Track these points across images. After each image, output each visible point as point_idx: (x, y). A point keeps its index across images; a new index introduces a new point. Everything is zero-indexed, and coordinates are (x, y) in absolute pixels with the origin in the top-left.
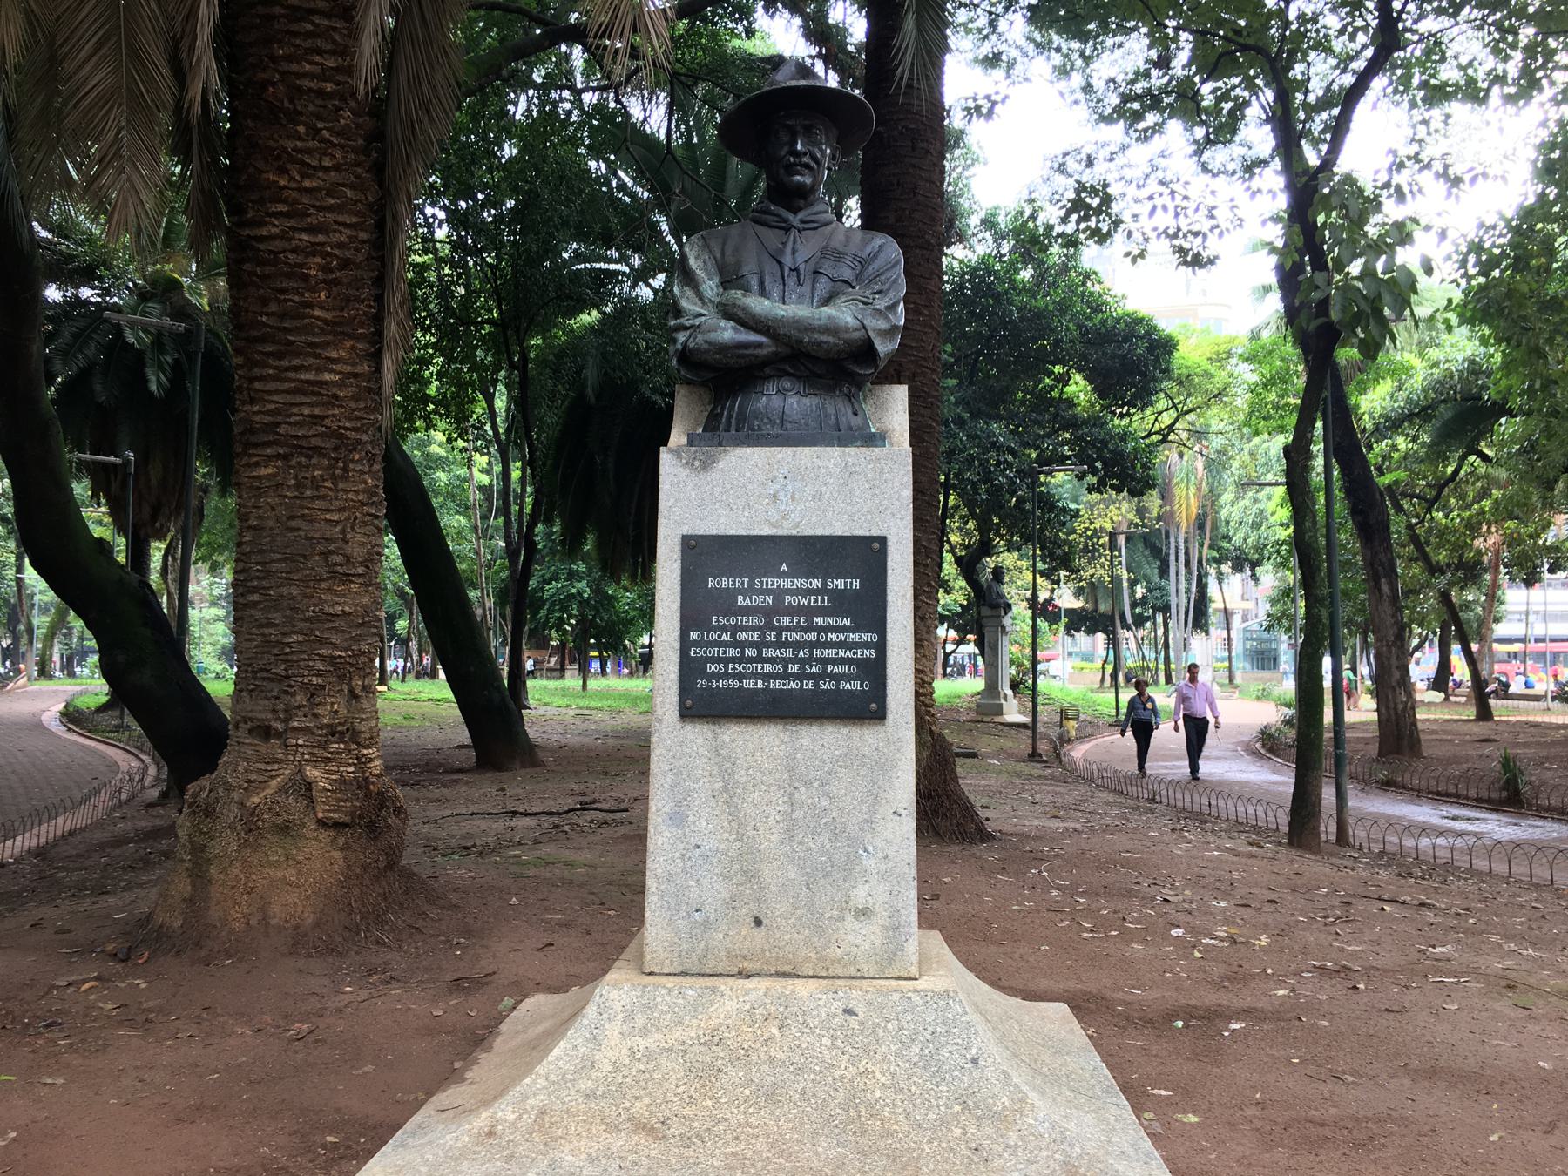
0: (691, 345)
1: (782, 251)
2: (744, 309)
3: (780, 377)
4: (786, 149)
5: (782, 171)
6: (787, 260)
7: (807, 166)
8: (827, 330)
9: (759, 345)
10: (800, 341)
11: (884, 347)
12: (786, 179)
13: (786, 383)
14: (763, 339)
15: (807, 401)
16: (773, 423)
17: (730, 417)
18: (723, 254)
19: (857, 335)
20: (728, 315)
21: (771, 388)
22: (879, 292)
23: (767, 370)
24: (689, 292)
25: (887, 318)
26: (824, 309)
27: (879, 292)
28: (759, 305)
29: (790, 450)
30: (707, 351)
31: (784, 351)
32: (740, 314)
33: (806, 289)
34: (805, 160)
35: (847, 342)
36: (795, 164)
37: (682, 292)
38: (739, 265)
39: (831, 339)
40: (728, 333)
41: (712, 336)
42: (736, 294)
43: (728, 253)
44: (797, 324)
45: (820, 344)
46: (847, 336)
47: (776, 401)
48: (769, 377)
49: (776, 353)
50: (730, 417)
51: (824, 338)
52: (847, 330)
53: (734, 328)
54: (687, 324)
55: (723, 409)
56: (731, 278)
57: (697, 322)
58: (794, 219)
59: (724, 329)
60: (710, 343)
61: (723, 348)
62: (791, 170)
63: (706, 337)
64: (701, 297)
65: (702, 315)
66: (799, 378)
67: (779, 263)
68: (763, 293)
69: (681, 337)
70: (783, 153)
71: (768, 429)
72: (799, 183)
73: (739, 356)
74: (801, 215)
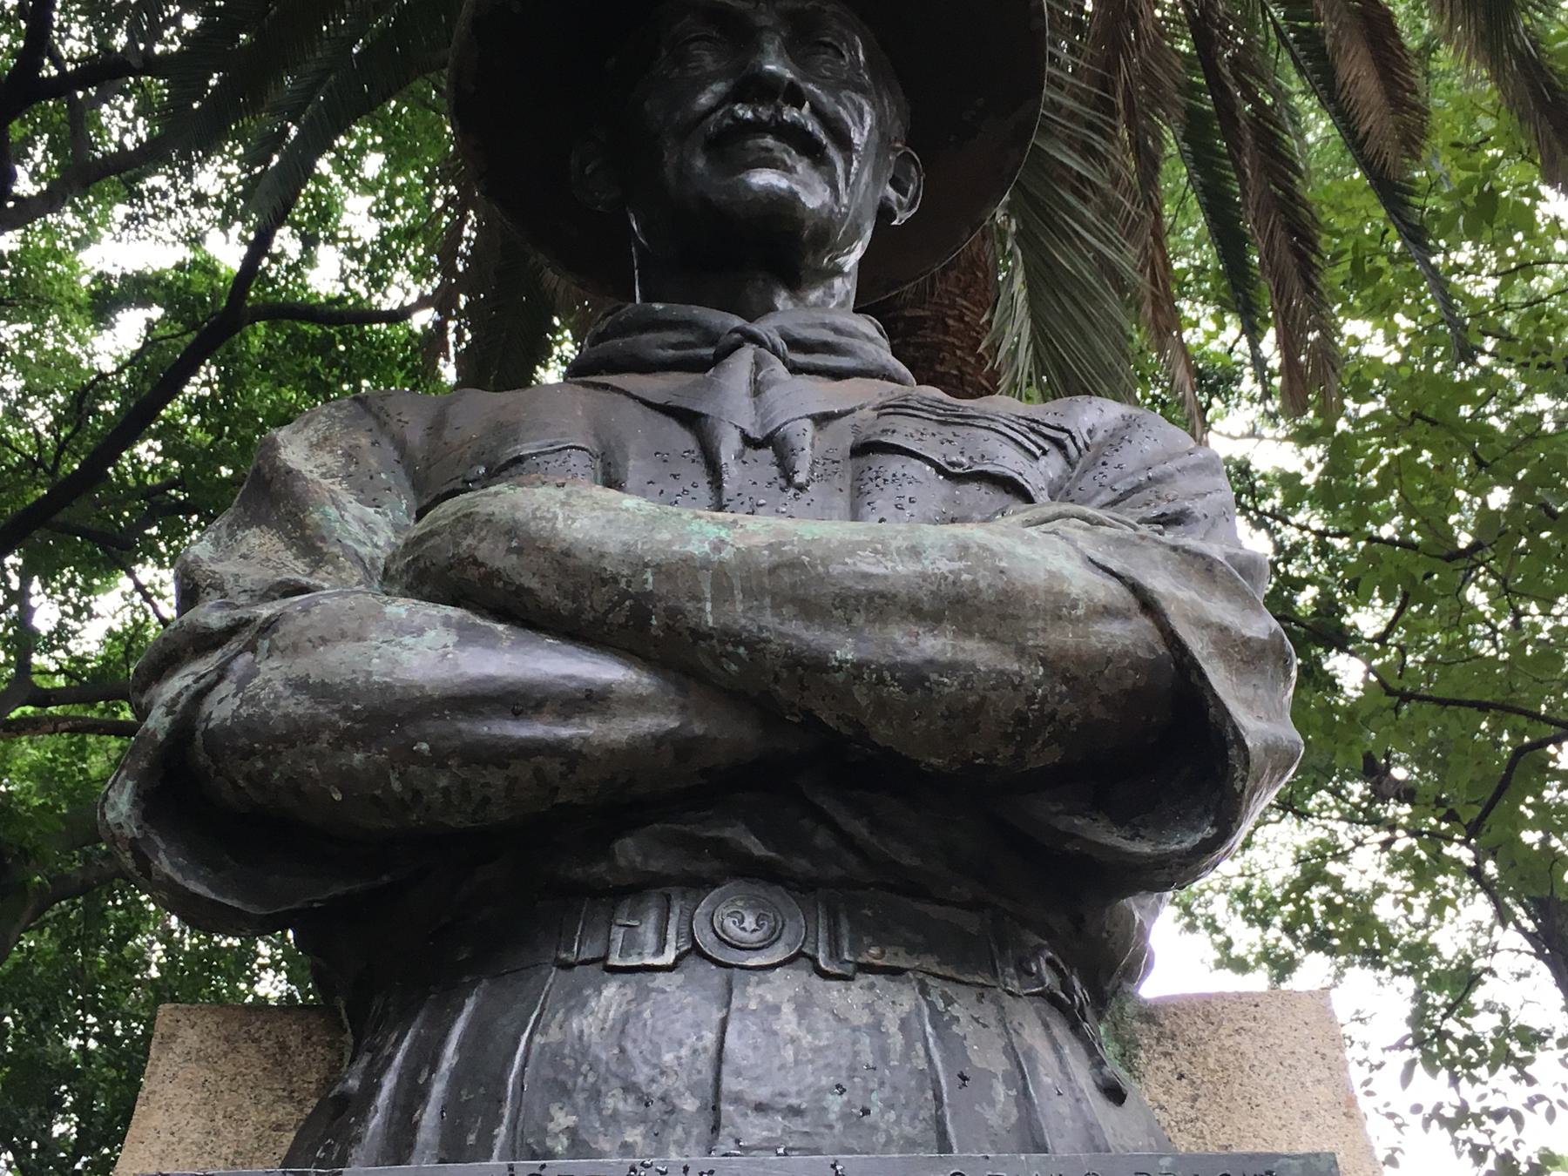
3: (697, 885)
8: (952, 606)
9: (592, 700)
15: (851, 998)
21: (648, 939)
30: (299, 734)
35: (1074, 673)
36: (757, 127)
41: (338, 661)
44: (796, 585)
45: (916, 677)
46: (1064, 638)
50: (412, 1096)
52: (1059, 608)
60: (321, 691)
61: (392, 715)
63: (303, 666)
66: (803, 888)
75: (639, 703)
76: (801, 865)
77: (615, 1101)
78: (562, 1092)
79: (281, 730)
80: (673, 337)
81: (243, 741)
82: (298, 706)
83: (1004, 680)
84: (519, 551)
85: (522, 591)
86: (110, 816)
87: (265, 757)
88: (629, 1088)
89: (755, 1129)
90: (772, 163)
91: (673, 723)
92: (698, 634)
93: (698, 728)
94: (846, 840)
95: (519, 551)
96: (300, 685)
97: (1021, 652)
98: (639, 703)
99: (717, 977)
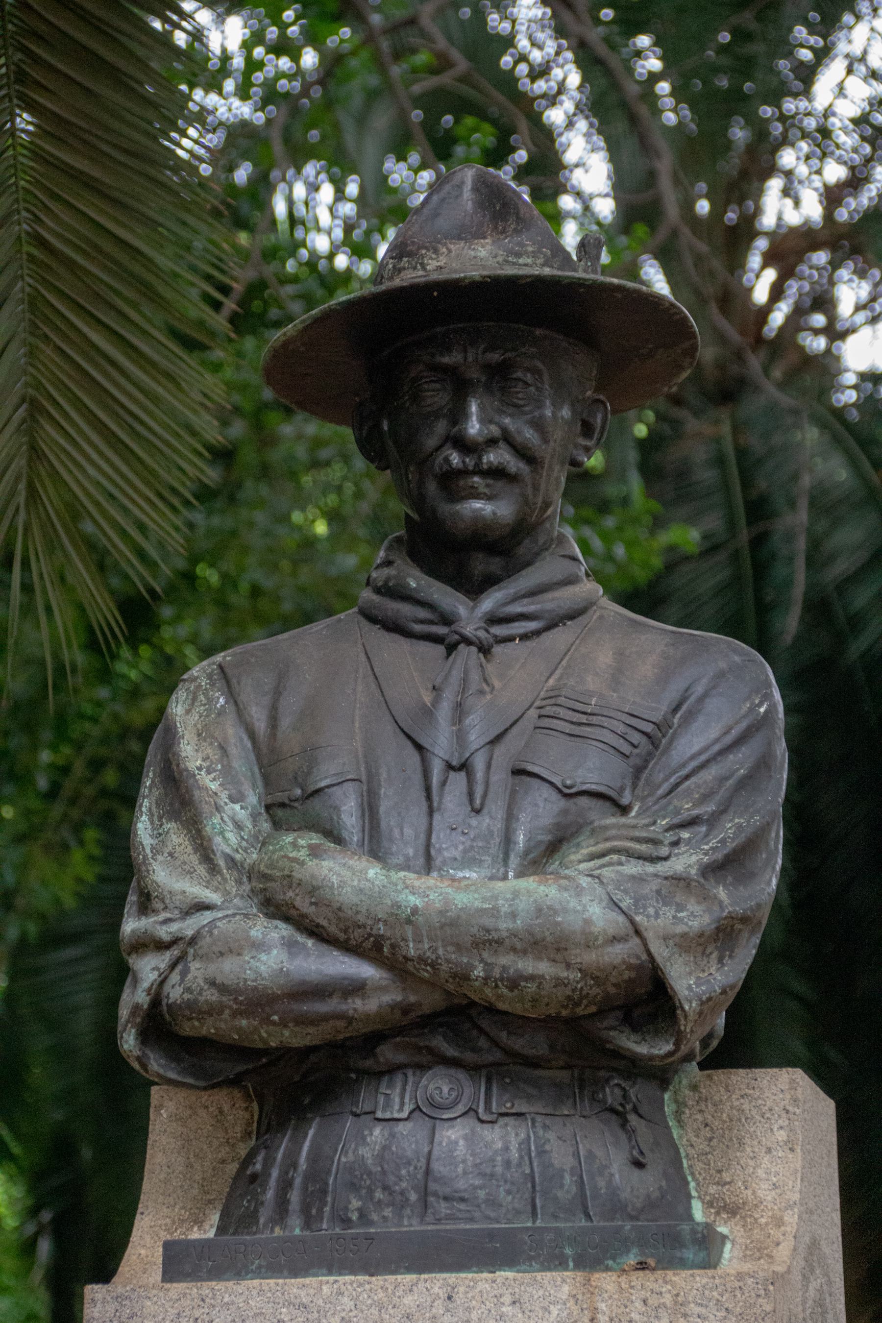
0: (175, 993)
1: (428, 713)
2: (313, 890)
3: (422, 1068)
4: (441, 427)
5: (432, 487)
6: (442, 744)
7: (498, 473)
8: (534, 944)
9: (356, 988)
10: (462, 977)
11: (699, 984)
12: (445, 509)
13: (439, 1084)
14: (366, 971)
16: (400, 1204)
17: (285, 1185)
18: (273, 721)
19: (617, 953)
20: (275, 908)
21: (396, 1098)
22: (692, 822)
23: (387, 1053)
24: (177, 838)
25: (705, 898)
26: (530, 883)
27: (692, 822)
28: (349, 877)
29: (437, 1283)
30: (213, 1011)
31: (430, 1001)
32: (304, 905)
33: (491, 821)
34: (492, 457)
36: (464, 472)
37: (159, 835)
38: (311, 754)
39: (543, 967)
40: (272, 956)
41: (229, 969)
42: (296, 845)
43: (285, 722)
45: (514, 983)
46: (590, 958)
47: (410, 1137)
48: (392, 1070)
49: (406, 1009)
50: (285, 1185)
51: (528, 965)
52: (589, 942)
53: (290, 945)
54: (164, 933)
55: (268, 1163)
56: (291, 804)
57: (188, 927)
58: (470, 614)
59: (259, 946)
60: (223, 989)
61: (257, 1002)
62: (452, 483)
64: (204, 851)
65: (203, 907)
66: (473, 1069)
67: (419, 747)
68: (375, 846)
69: (148, 968)
70: (431, 442)
71: (387, 1223)
72: (477, 517)
73: (303, 1021)
74: (489, 602)
75: (383, 989)
76: (469, 1057)
77: (379, 1195)
78: (354, 1187)
79: (205, 1008)
80: (422, 613)
81: (187, 1012)
82: (211, 996)
83: (559, 983)
84: (315, 904)
85: (318, 926)
86: (126, 1047)
87: (198, 1020)
88: (385, 1188)
89: (443, 1208)
90: (477, 496)
91: (399, 998)
92: (407, 959)
93: (412, 999)
94: (496, 1043)
95: (315, 904)
96: (212, 983)
97: (568, 966)
98: (383, 989)
99: (428, 1122)
